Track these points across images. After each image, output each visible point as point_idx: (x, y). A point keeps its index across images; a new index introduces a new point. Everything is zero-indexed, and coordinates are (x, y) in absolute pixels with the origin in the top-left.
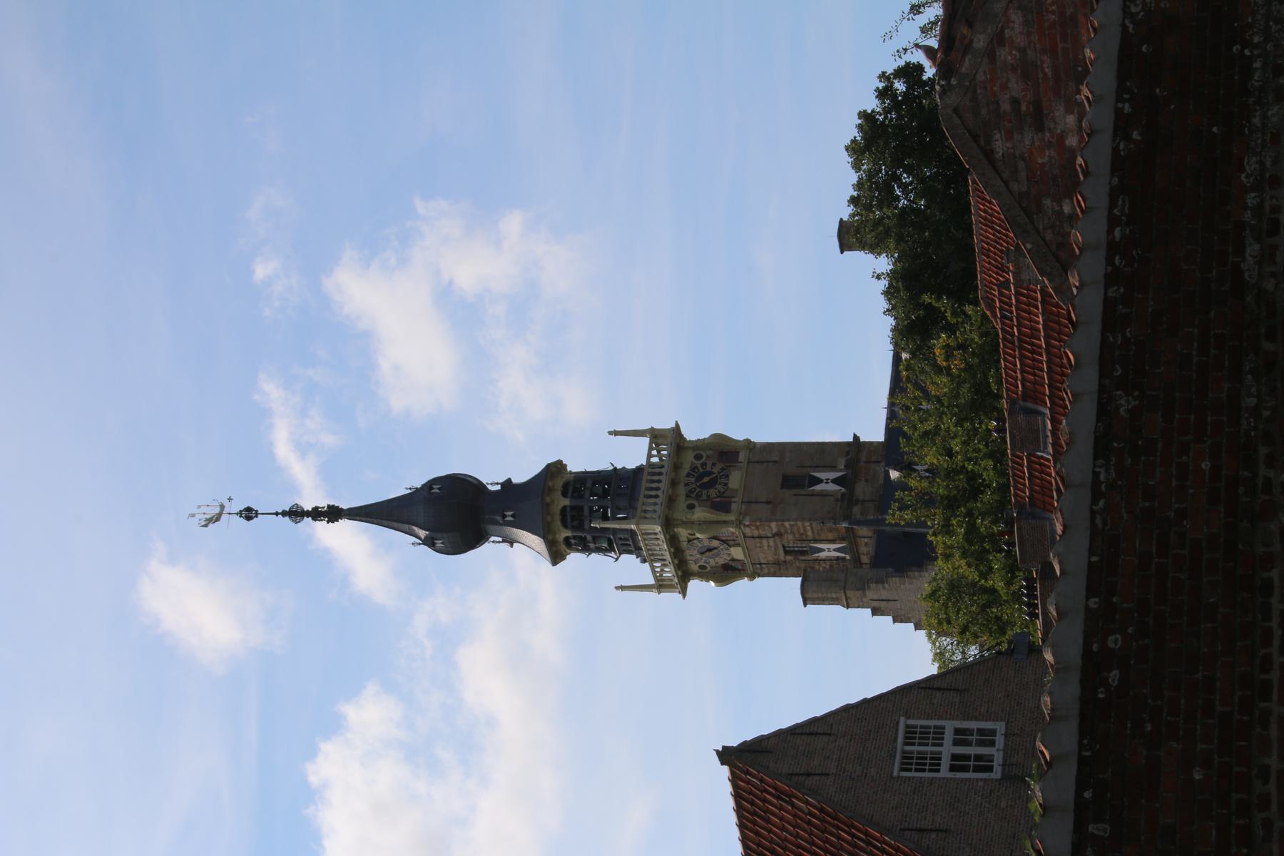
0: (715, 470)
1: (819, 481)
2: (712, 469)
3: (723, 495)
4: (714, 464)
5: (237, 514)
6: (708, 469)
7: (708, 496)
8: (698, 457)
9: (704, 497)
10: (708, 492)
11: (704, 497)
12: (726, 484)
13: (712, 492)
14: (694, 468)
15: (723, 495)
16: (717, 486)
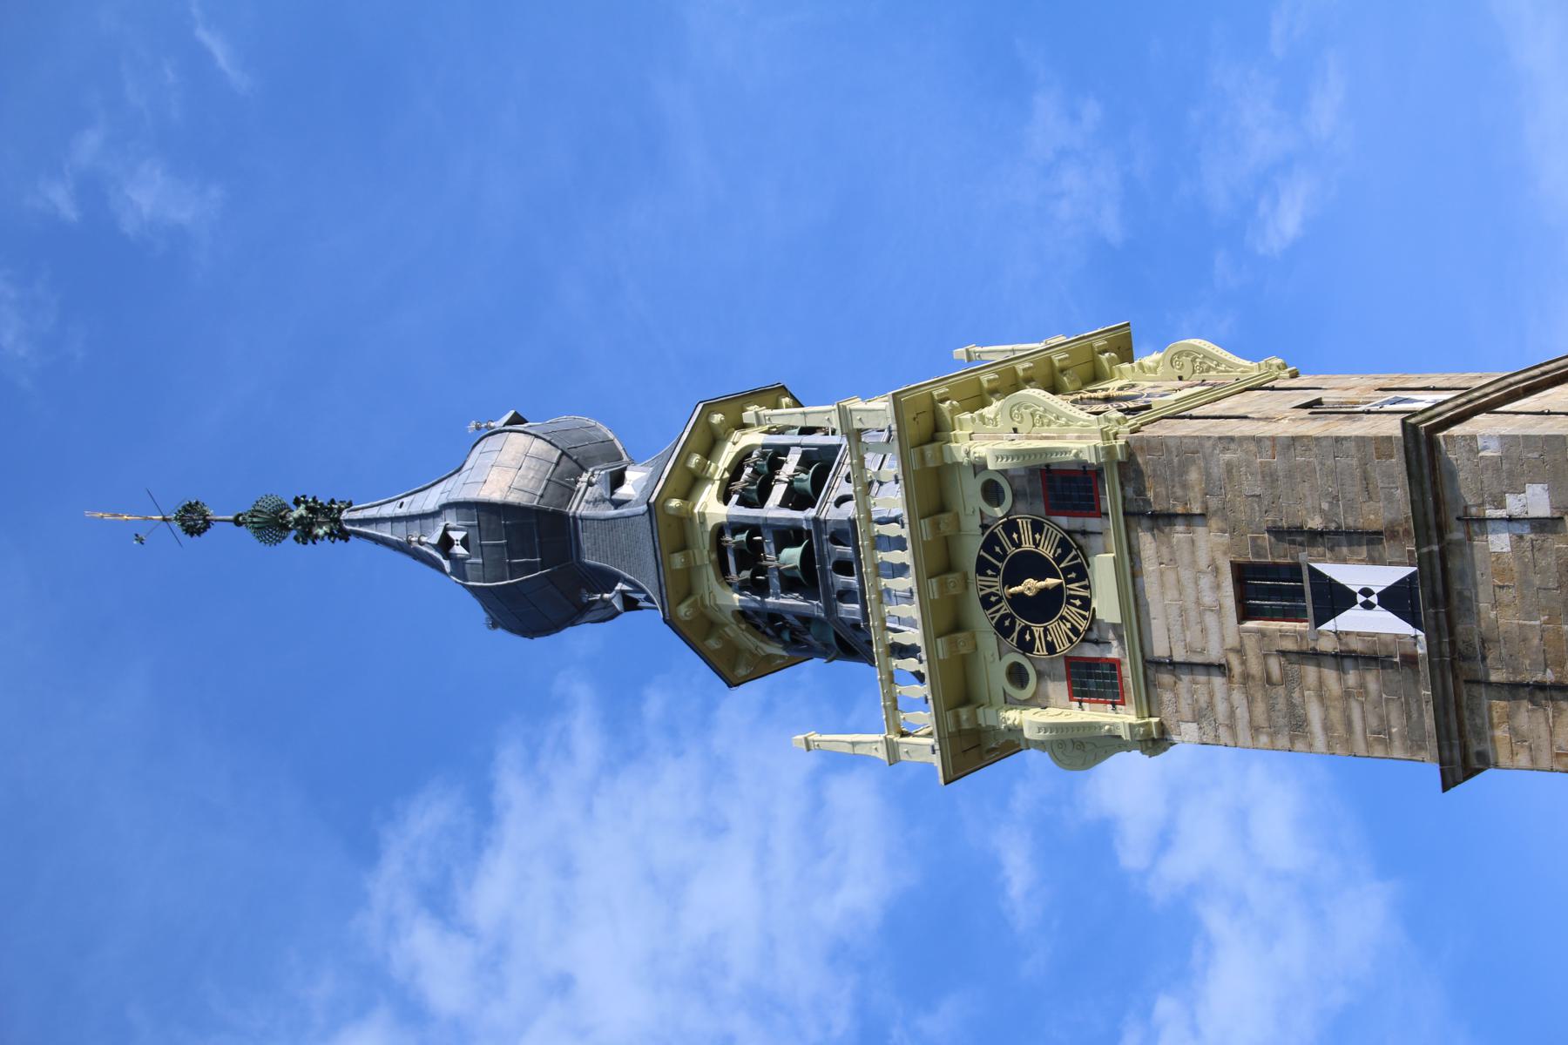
0: (1047, 551)
1: (1336, 599)
2: (1037, 546)
3: (1094, 635)
4: (1037, 527)
5: (176, 519)
6: (1028, 546)
7: (1051, 648)
8: (992, 492)
9: (1041, 651)
10: (1046, 630)
11: (1041, 651)
12: (1086, 603)
13: (1058, 630)
14: (991, 543)
15: (1094, 635)
16: (1064, 611)
